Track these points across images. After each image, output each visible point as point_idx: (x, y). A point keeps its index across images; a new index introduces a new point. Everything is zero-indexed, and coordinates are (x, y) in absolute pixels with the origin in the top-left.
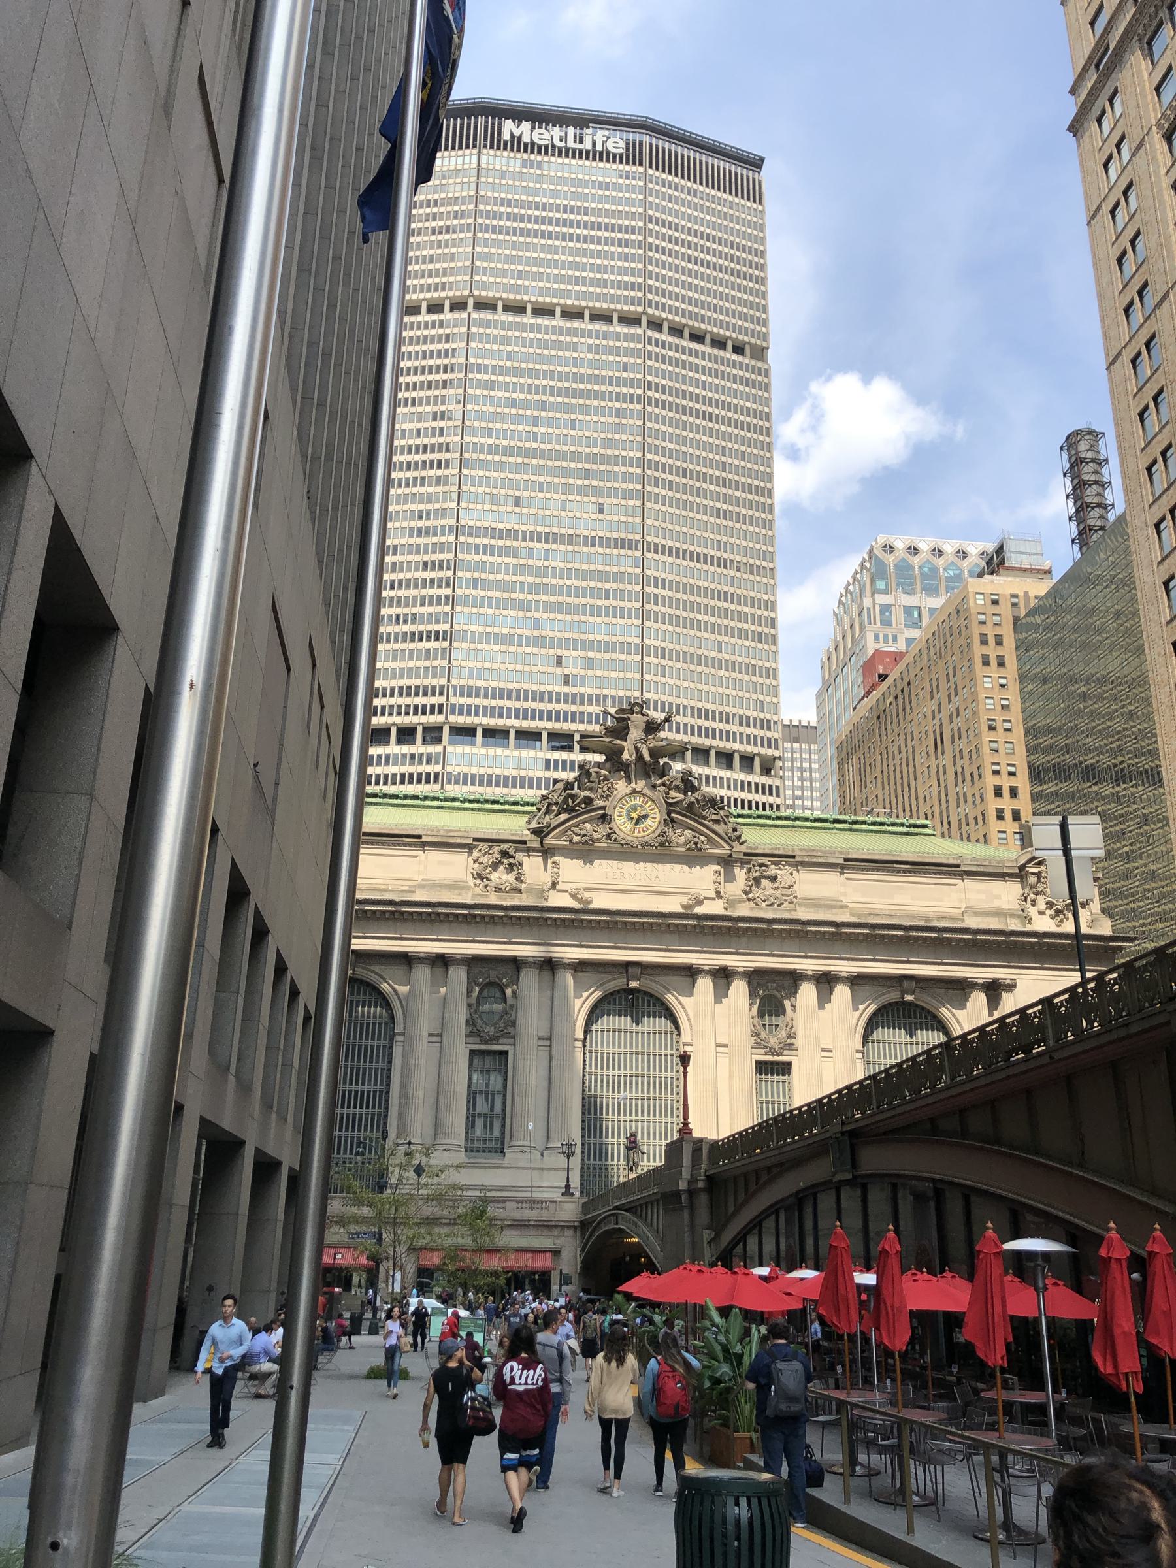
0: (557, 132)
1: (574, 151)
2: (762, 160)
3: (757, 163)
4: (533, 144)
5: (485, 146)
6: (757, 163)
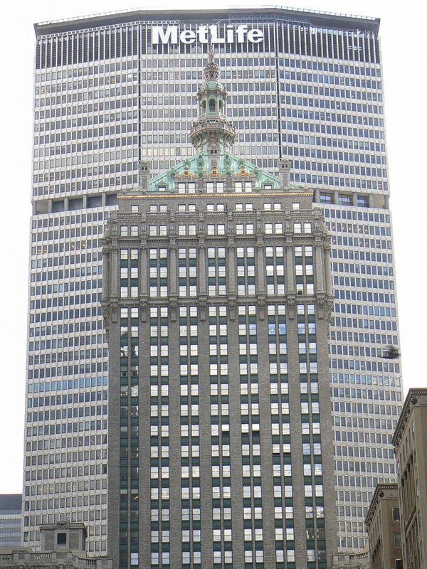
0: (202, 30)
1: (216, 45)
2: (378, 20)
3: (371, 26)
4: (182, 44)
5: (144, 53)
6: (371, 26)
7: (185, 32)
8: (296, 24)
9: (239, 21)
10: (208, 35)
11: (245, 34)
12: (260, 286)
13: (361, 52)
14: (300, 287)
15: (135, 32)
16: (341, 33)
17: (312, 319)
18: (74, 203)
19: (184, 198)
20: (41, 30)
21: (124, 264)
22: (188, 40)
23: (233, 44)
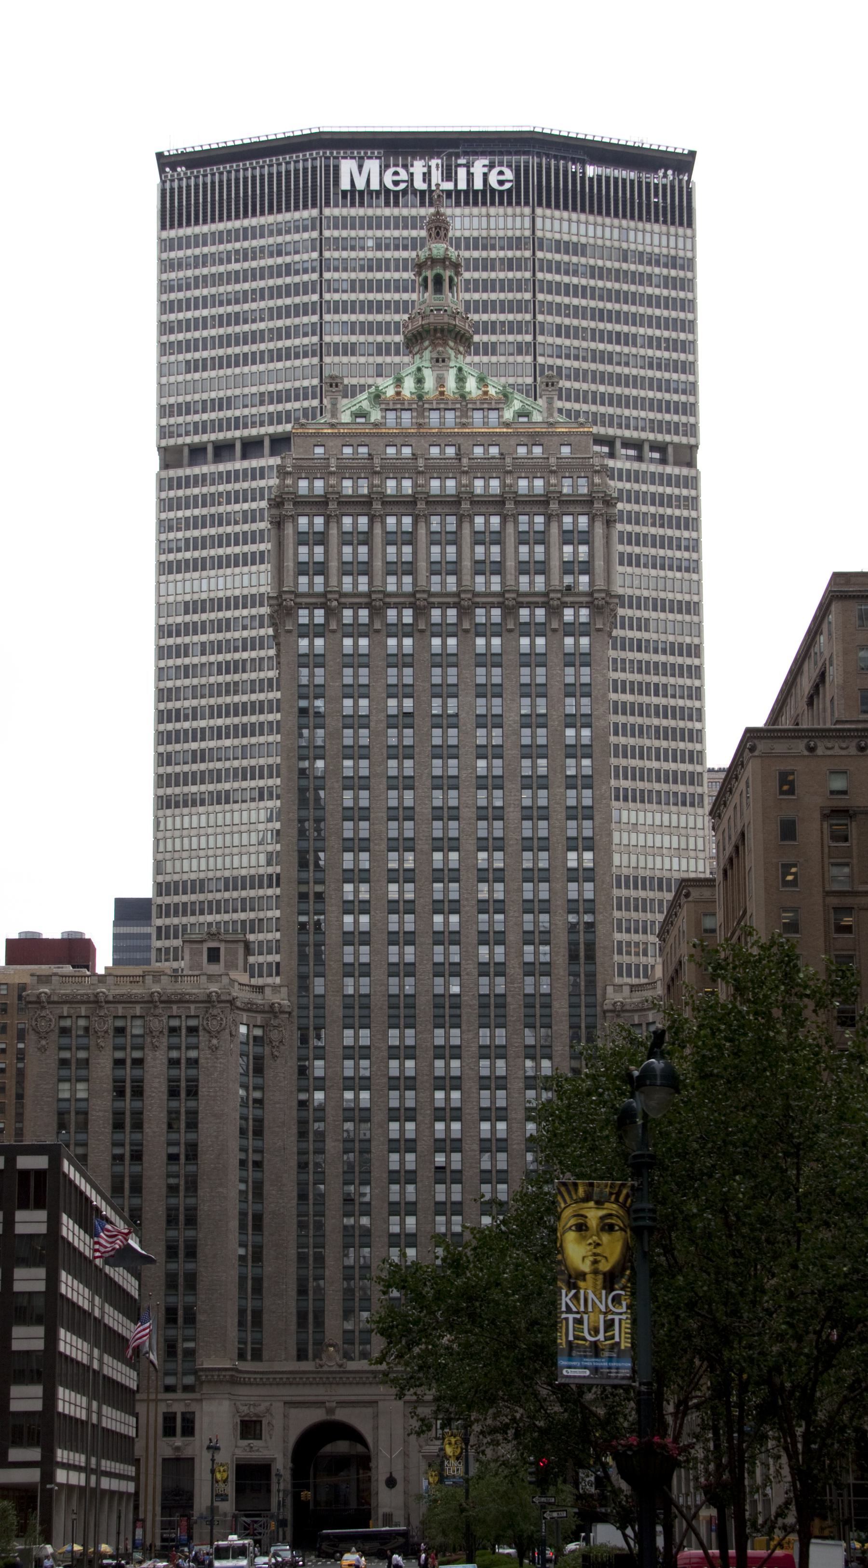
0: (418, 167)
3: (683, 163)
4: (387, 191)
5: (328, 204)
6: (683, 163)
7: (392, 170)
8: (564, 158)
9: (476, 154)
10: (427, 177)
11: (485, 175)
12: (508, 577)
13: (665, 208)
14: (568, 580)
15: (314, 168)
16: (633, 175)
17: (584, 630)
19: (395, 435)
20: (165, 161)
21: (302, 539)
22: (396, 183)
23: (466, 192)
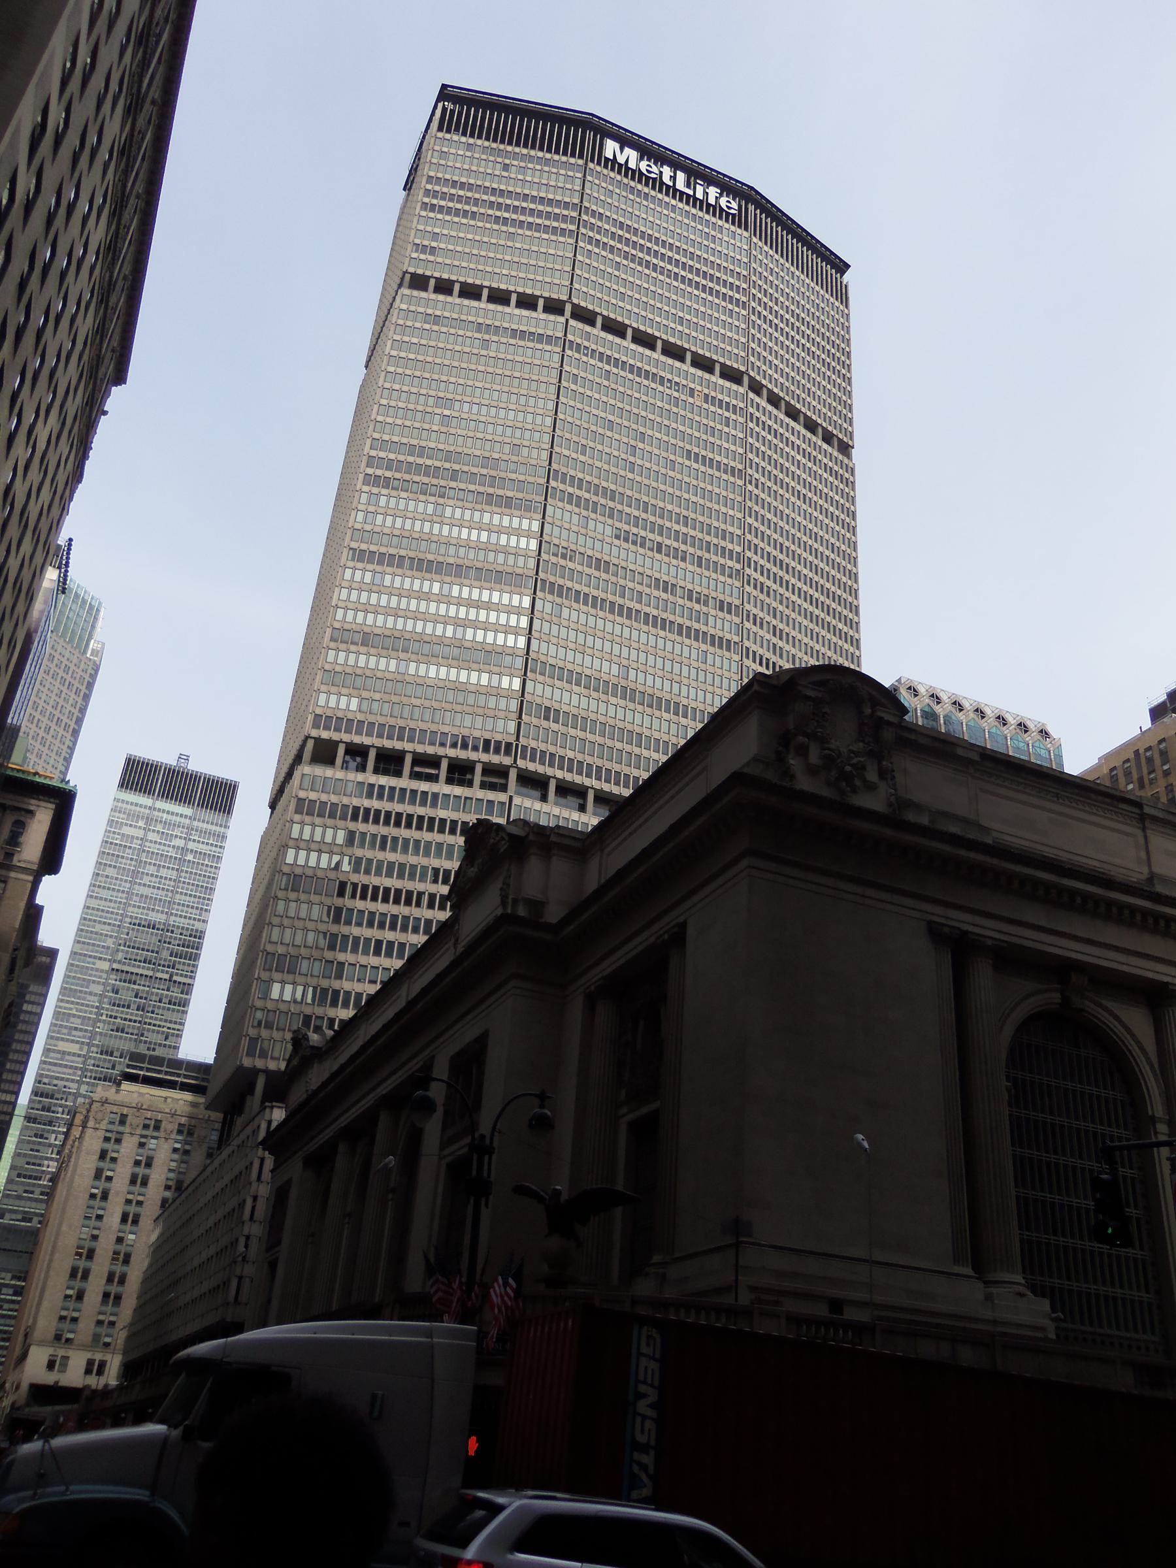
0: (667, 171)
1: (682, 193)
3: (841, 267)
5: (592, 161)
10: (674, 178)
18: (471, 292)
20: (445, 94)
